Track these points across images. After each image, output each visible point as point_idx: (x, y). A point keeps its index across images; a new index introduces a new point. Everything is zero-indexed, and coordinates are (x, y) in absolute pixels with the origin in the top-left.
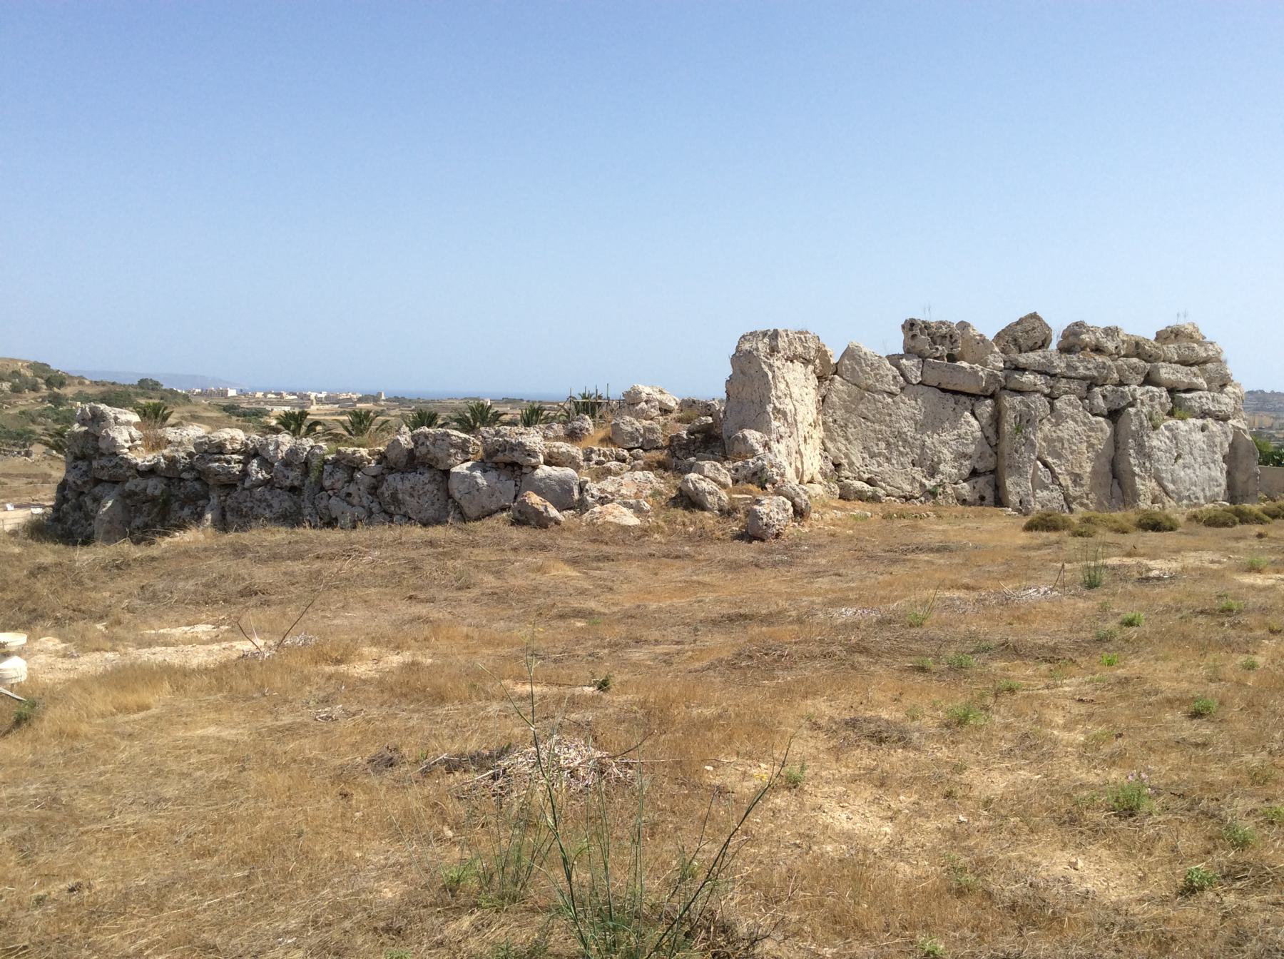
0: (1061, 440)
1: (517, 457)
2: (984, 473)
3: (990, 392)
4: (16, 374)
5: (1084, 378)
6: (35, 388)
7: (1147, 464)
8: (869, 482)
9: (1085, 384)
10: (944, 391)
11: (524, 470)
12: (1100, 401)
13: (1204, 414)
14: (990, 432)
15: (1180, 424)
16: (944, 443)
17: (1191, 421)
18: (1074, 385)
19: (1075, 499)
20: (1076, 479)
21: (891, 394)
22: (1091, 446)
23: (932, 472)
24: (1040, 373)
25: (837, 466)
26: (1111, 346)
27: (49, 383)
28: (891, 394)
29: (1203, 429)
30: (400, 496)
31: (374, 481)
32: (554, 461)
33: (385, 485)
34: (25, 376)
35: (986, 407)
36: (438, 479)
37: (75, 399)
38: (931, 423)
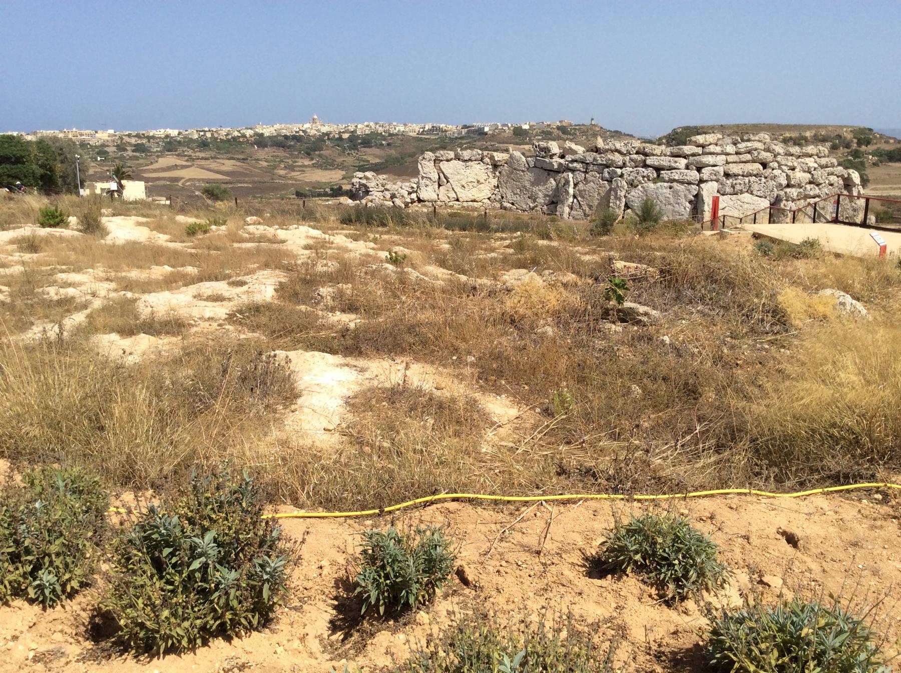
0: (585, 191)
4: (839, 136)
5: (601, 165)
6: (847, 146)
7: (618, 202)
8: (513, 204)
12: (606, 175)
15: (652, 185)
16: (540, 190)
17: (659, 184)
20: (590, 207)
21: (523, 171)
22: (599, 194)
23: (535, 201)
24: (582, 162)
25: (502, 197)
27: (859, 143)
28: (523, 171)
29: (671, 188)
34: (845, 138)
37: (869, 154)
38: (534, 183)
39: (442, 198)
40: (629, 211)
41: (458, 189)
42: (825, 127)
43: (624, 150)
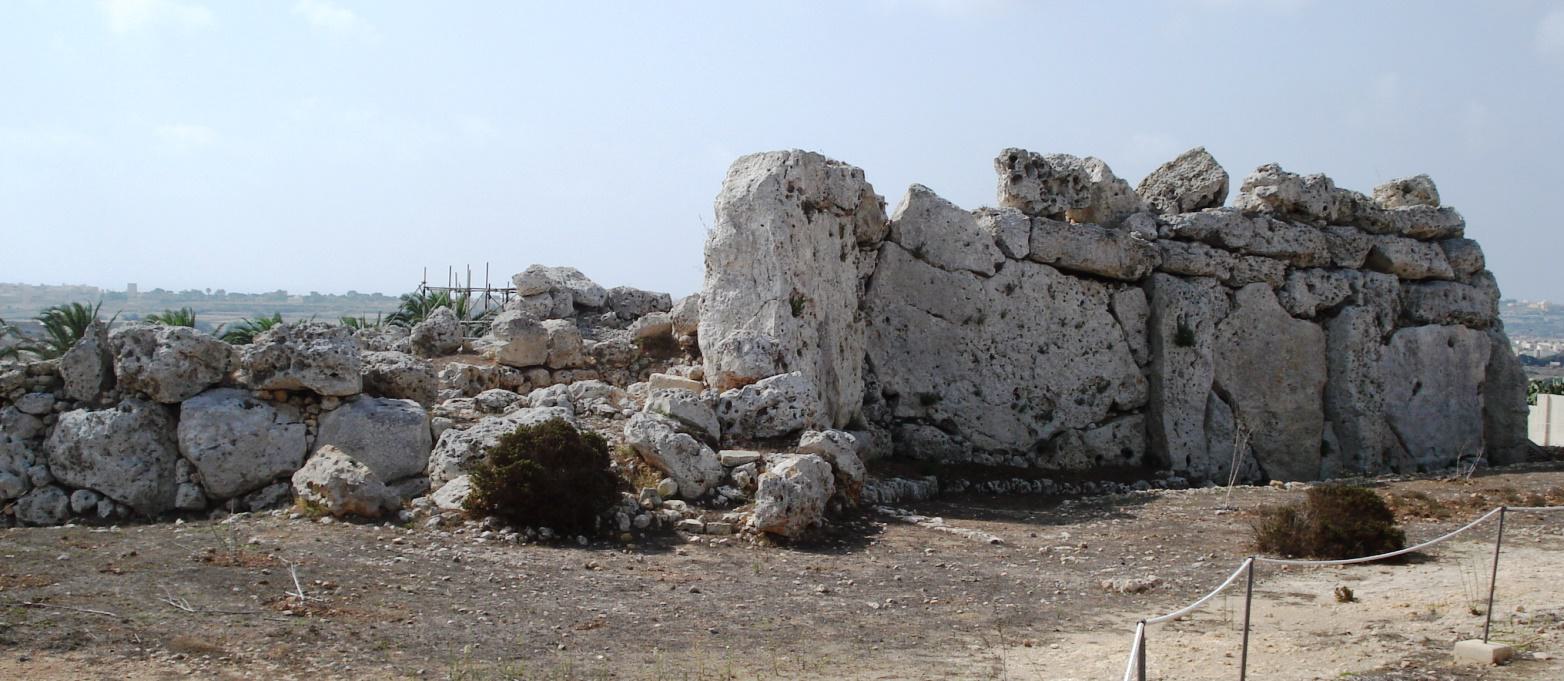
2: (1130, 412)
9: (1281, 267)
11: (326, 404)
13: (1455, 317)
14: (1138, 342)
18: (1266, 266)
19: (1269, 454)
26: (1316, 208)
29: (1451, 344)
30: (85, 453)
31: (36, 424)
32: (383, 387)
33: (58, 431)
35: (1131, 301)
36: (161, 421)
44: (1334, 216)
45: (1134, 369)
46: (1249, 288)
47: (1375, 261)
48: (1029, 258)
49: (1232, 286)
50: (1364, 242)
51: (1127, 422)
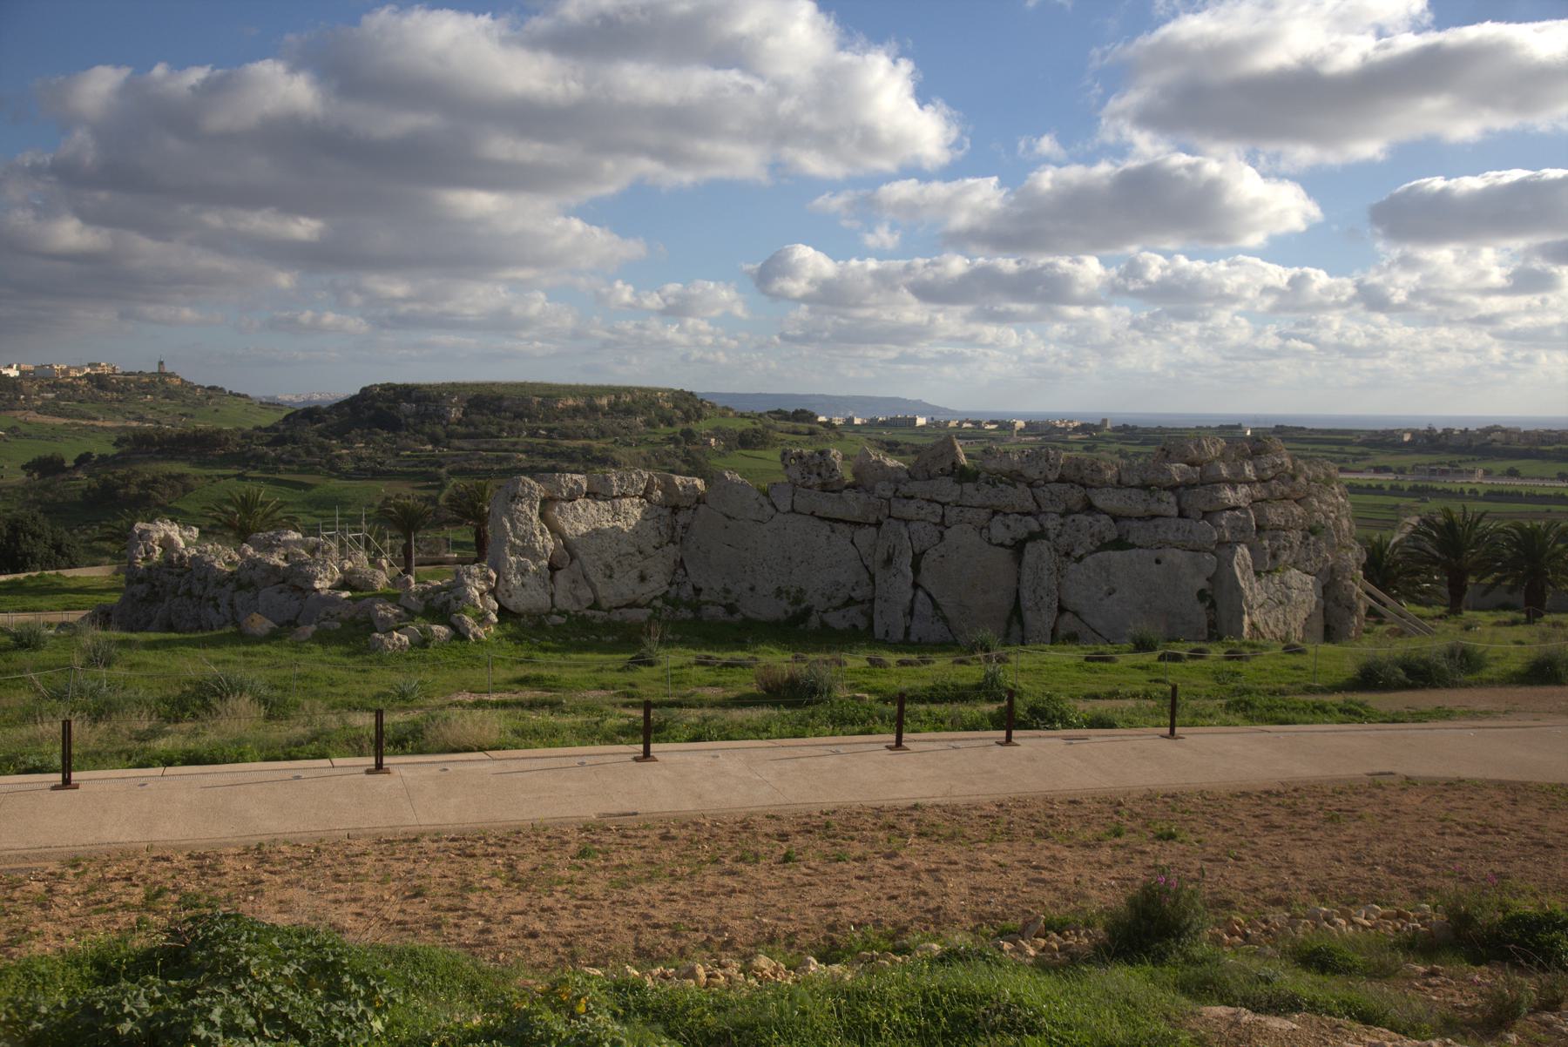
1: (298, 582)
3: (872, 519)
6: (670, 424)
9: (984, 514)
10: (820, 518)
18: (969, 514)
29: (1158, 562)
35: (865, 536)
39: (563, 602)
40: (1068, 617)
41: (597, 578)
42: (629, 390)
43: (1032, 473)
44: (1052, 476)
45: (865, 576)
46: (954, 528)
47: (1090, 508)
48: (793, 511)
49: (943, 524)
50: (1075, 495)
51: (853, 611)
